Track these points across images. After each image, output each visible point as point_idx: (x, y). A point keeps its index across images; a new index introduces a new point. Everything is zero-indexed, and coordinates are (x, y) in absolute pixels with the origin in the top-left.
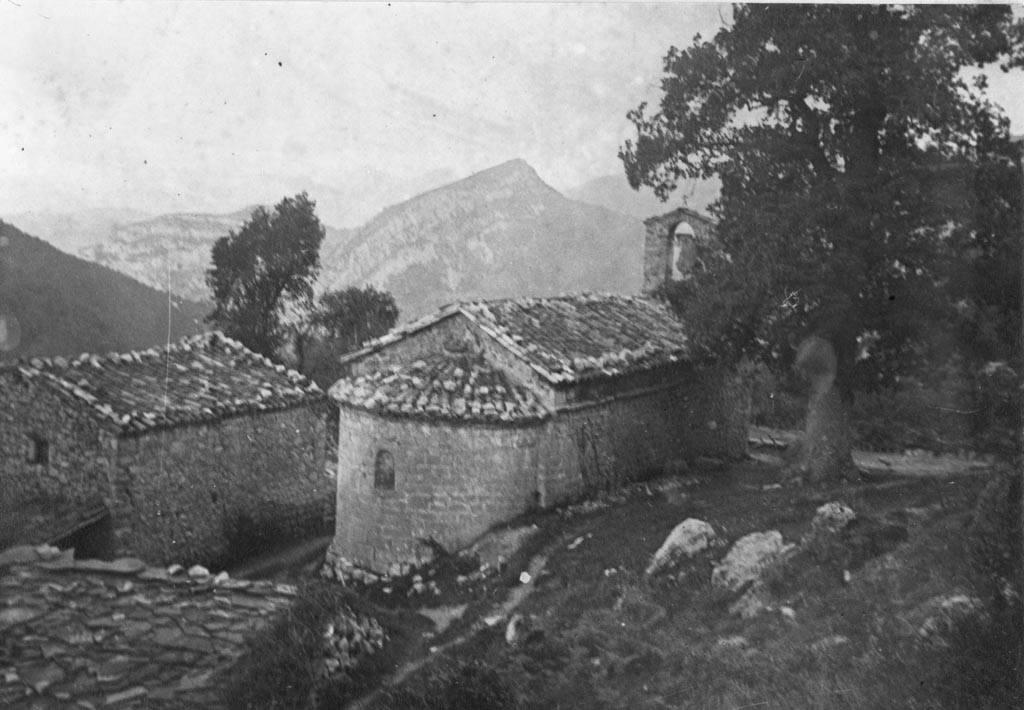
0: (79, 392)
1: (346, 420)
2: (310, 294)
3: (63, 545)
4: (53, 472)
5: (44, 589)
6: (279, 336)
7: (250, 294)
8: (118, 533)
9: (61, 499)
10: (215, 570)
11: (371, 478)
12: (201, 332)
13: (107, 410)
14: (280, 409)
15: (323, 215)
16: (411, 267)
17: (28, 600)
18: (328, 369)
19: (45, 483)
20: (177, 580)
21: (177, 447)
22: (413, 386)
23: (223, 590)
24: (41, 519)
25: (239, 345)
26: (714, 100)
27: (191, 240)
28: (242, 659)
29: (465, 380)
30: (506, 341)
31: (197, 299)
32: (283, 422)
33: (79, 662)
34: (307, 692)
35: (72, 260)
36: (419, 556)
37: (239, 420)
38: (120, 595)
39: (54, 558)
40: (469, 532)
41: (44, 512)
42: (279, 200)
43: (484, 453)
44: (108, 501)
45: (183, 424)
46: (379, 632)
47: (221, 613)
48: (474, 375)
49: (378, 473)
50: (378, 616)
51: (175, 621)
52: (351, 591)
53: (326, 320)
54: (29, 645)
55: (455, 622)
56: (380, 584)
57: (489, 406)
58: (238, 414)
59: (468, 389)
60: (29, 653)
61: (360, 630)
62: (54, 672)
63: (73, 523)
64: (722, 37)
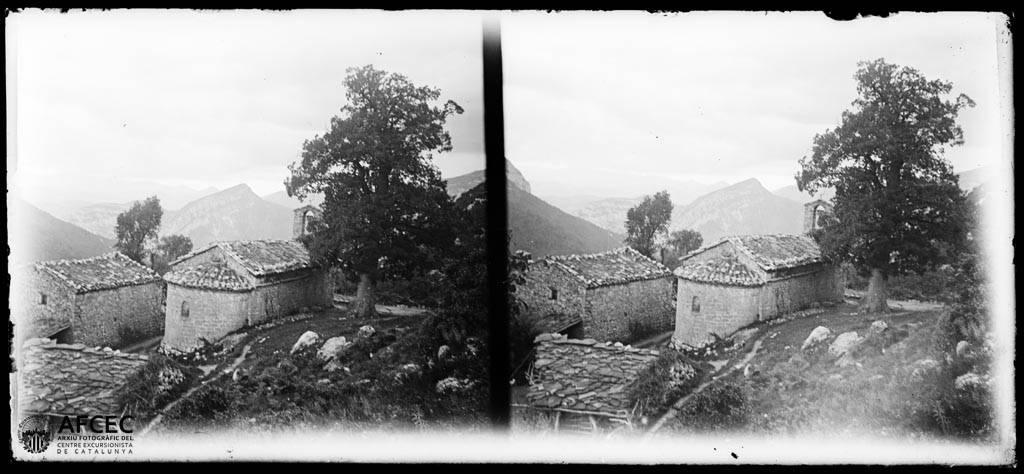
0: (570, 270)
1: (680, 282)
2: (667, 232)
3: (562, 333)
4: (559, 303)
5: (554, 351)
6: (654, 249)
7: (642, 231)
8: (586, 328)
9: (562, 314)
10: (625, 344)
11: (690, 308)
12: (621, 246)
13: (582, 278)
14: (653, 279)
15: (673, 200)
16: (709, 222)
17: (548, 356)
18: (672, 263)
19: (555, 307)
20: (610, 348)
21: (611, 294)
22: (708, 271)
23: (629, 353)
24: (554, 322)
25: (637, 252)
26: (834, 156)
27: (618, 209)
28: (636, 380)
29: (730, 268)
30: (747, 252)
31: (620, 233)
32: (655, 284)
33: (568, 381)
34: (662, 394)
35: (569, 216)
36: (709, 340)
37: (637, 283)
38: (586, 354)
39: (559, 338)
40: (729, 331)
41: (555, 319)
42: (655, 194)
43: (737, 298)
44: (581, 315)
45: (613, 284)
46: (693, 370)
47: (627, 362)
48: (733, 266)
49: (693, 305)
50: (692, 364)
51: (608, 365)
52: (681, 354)
53: (674, 243)
54: (548, 375)
55: (723, 367)
56: (693, 351)
57: (739, 279)
58: (637, 280)
59: (731, 272)
60: (548, 378)
61: (684, 369)
62: (558, 386)
63: (567, 324)
64: (838, 130)
